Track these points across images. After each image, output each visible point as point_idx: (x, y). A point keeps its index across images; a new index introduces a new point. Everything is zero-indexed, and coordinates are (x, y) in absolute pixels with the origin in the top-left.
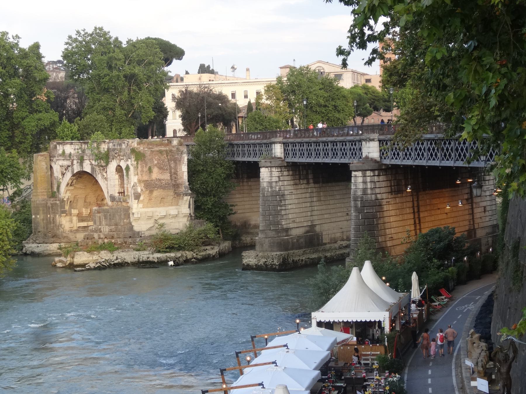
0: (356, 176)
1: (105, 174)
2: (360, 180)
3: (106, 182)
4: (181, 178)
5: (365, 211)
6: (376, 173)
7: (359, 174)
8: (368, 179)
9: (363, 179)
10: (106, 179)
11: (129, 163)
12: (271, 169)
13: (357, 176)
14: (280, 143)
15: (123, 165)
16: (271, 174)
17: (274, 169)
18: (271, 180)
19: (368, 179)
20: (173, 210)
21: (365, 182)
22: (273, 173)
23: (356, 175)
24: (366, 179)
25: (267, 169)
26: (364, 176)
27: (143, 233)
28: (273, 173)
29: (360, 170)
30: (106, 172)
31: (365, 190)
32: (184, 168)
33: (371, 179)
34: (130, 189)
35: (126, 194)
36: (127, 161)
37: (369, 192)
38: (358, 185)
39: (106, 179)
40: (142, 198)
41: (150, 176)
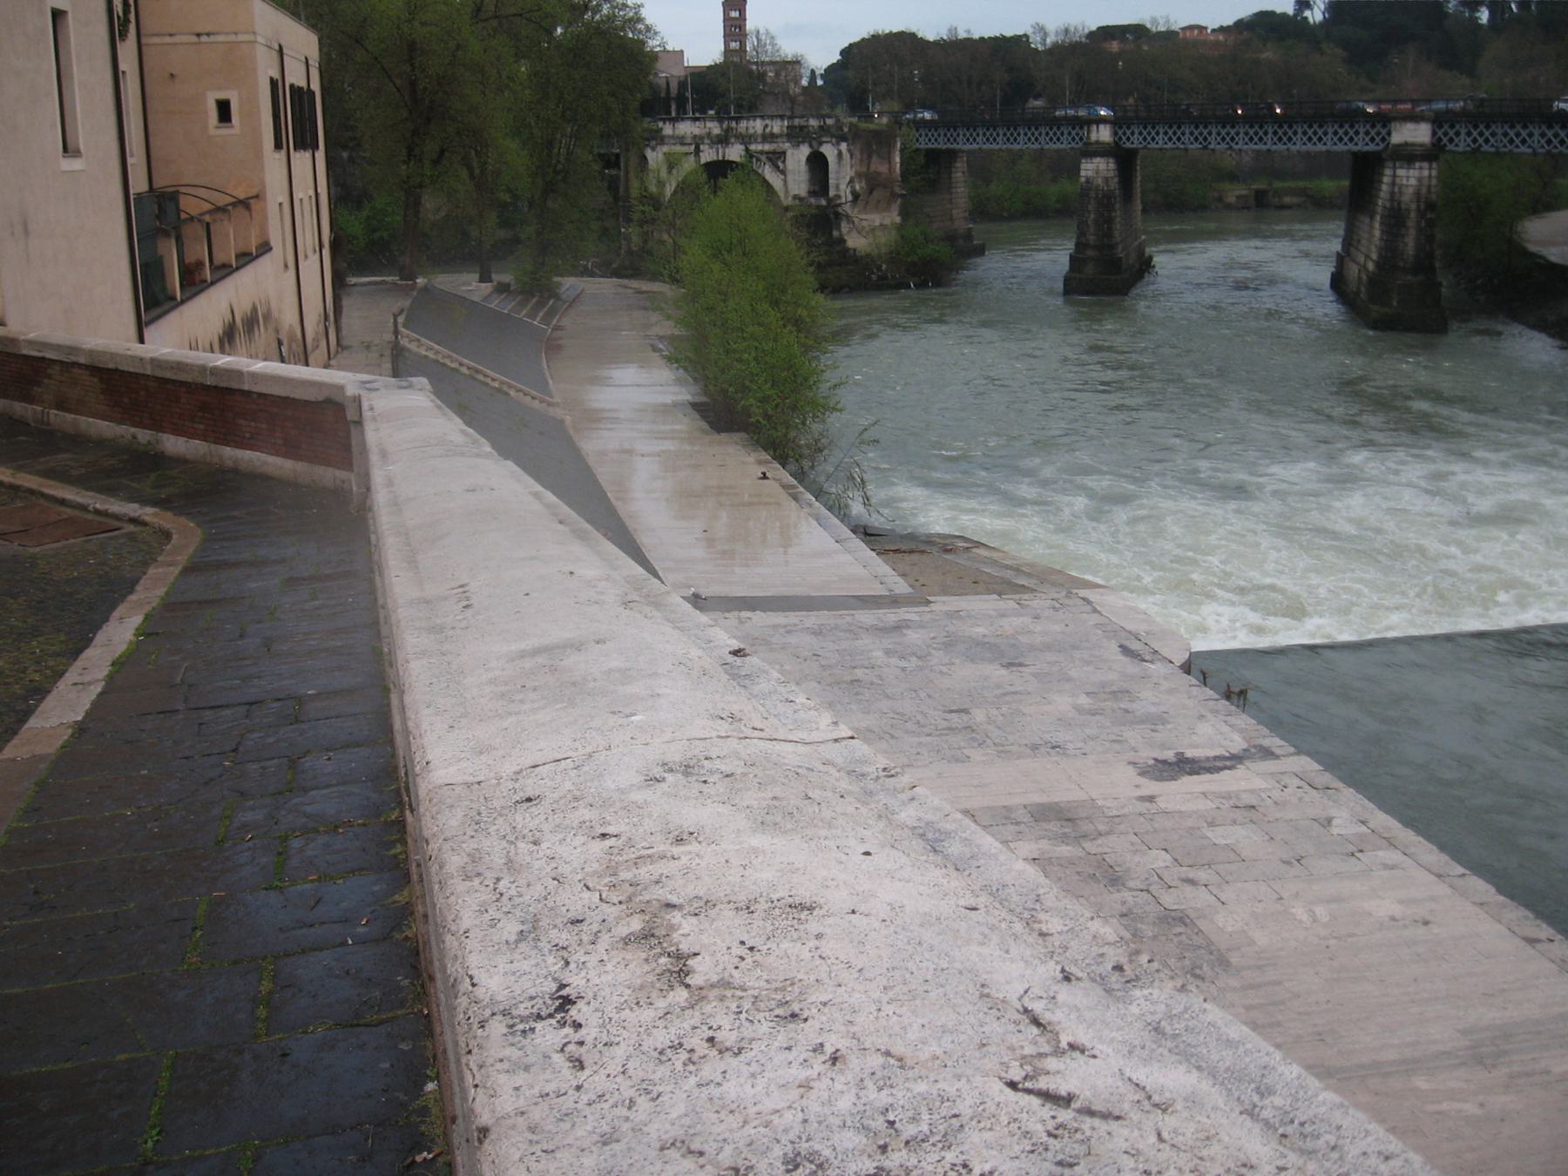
1: (780, 164)
3: (783, 177)
4: (895, 171)
7: (1425, 165)
10: (783, 172)
11: (844, 146)
15: (829, 151)
17: (1111, 160)
26: (1430, 168)
30: (784, 162)
32: (898, 159)
34: (843, 187)
35: (832, 193)
36: (838, 144)
39: (783, 172)
41: (868, 168)
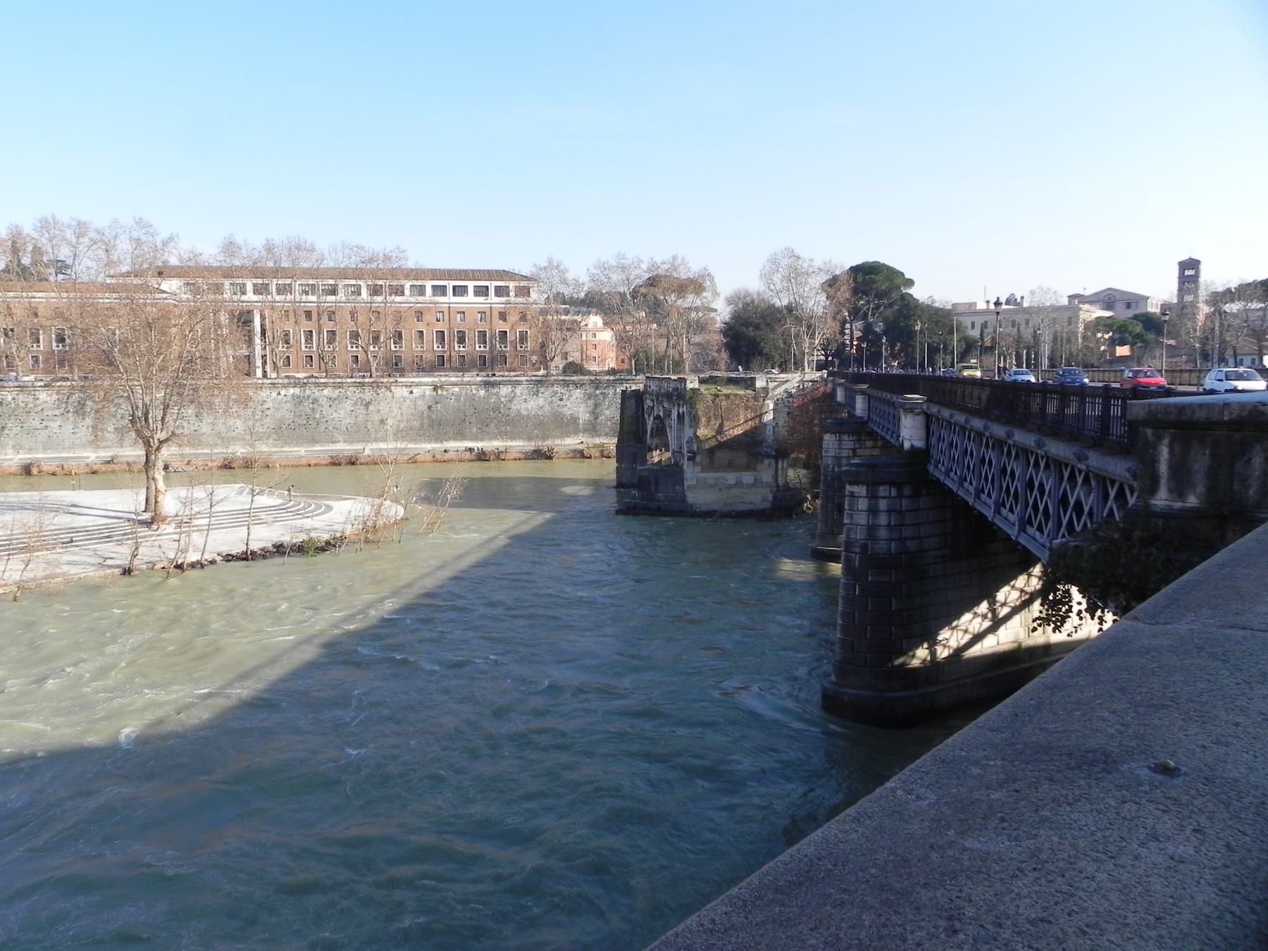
0: (852, 495)
2: (863, 504)
5: (870, 579)
6: (907, 491)
7: (861, 490)
8: (883, 504)
9: (870, 504)
12: (840, 436)
13: (856, 495)
14: (863, 392)
16: (840, 444)
17: (845, 437)
18: (839, 453)
19: (883, 504)
20: (747, 478)
21: (873, 511)
22: (844, 443)
23: (853, 492)
24: (877, 504)
25: (833, 436)
26: (873, 496)
27: (698, 506)
28: (844, 443)
29: (862, 483)
31: (871, 529)
33: (888, 506)
37: (883, 533)
38: (855, 516)
40: (698, 459)
